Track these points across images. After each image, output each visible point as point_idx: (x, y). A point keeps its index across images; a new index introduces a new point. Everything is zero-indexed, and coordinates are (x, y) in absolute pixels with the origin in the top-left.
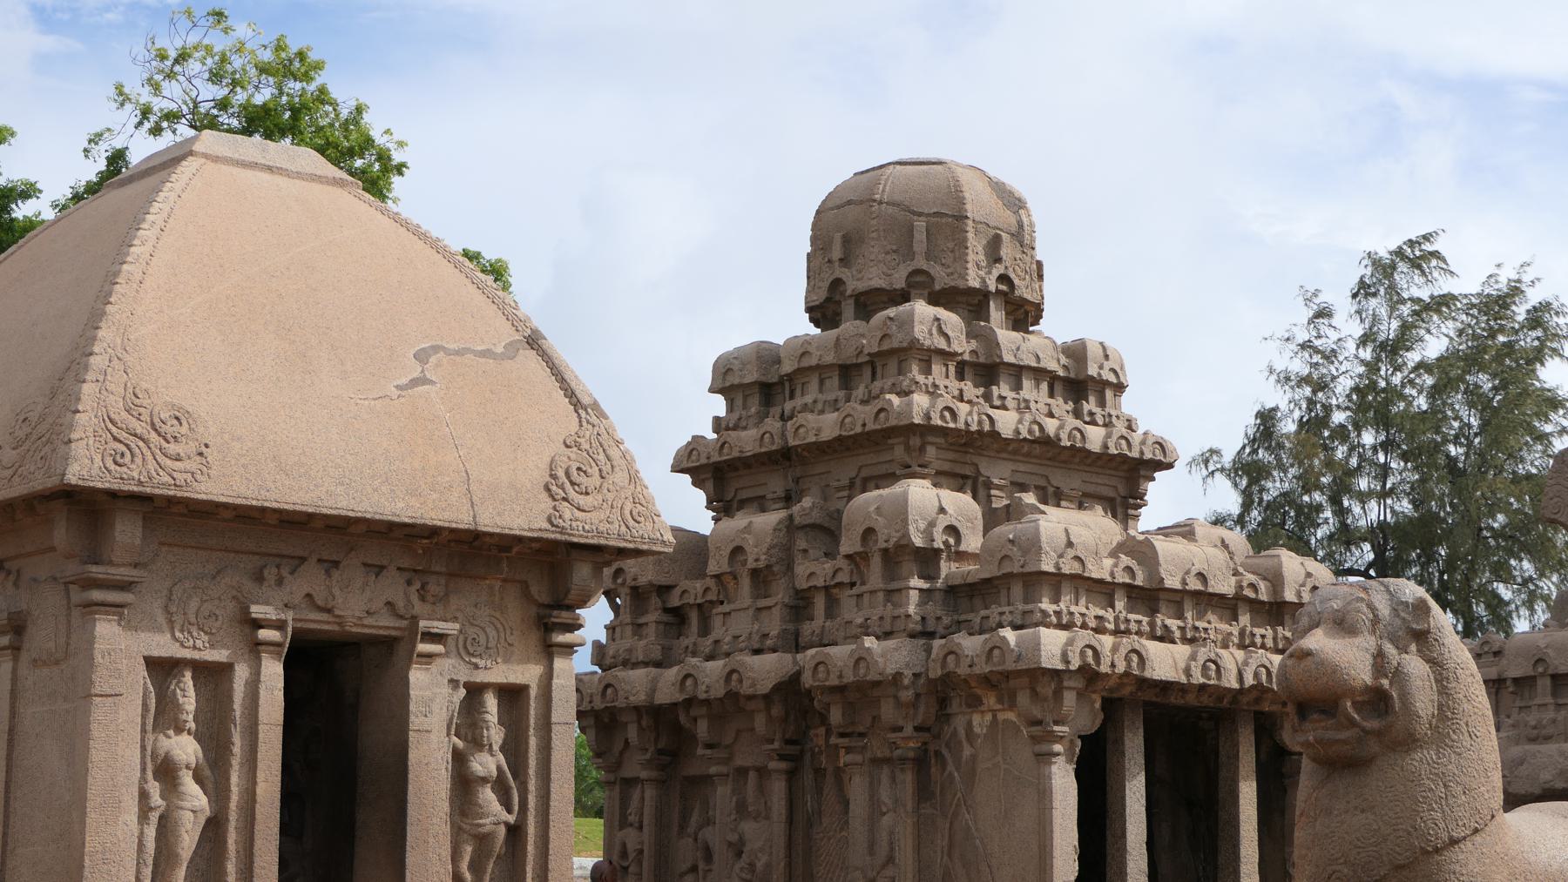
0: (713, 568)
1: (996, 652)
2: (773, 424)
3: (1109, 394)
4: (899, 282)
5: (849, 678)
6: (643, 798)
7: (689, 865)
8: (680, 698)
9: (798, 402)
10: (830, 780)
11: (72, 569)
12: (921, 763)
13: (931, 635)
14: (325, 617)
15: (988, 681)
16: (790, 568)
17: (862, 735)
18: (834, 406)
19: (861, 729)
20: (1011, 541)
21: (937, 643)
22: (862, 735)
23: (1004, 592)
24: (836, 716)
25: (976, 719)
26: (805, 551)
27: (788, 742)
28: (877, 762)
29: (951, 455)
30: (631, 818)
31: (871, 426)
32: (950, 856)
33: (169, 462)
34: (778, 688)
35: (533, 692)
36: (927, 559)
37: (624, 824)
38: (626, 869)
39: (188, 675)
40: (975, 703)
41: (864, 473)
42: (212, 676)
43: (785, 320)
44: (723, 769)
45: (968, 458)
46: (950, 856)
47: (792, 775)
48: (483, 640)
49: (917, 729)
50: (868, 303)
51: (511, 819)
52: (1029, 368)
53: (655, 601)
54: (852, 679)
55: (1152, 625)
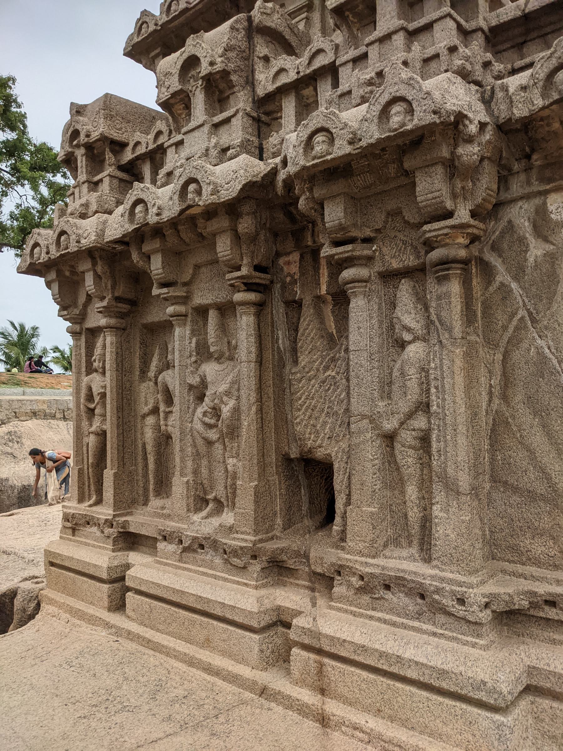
6: (104, 346)
7: (150, 406)
8: (130, 228)
17: (367, 240)
19: (368, 233)
22: (367, 240)
24: (334, 214)
26: (266, 59)
28: (390, 277)
30: (96, 364)
32: (505, 397)
37: (90, 370)
38: (93, 410)
44: (181, 309)
46: (505, 397)
47: (260, 308)
49: (474, 214)
53: (109, 156)
54: (377, 135)
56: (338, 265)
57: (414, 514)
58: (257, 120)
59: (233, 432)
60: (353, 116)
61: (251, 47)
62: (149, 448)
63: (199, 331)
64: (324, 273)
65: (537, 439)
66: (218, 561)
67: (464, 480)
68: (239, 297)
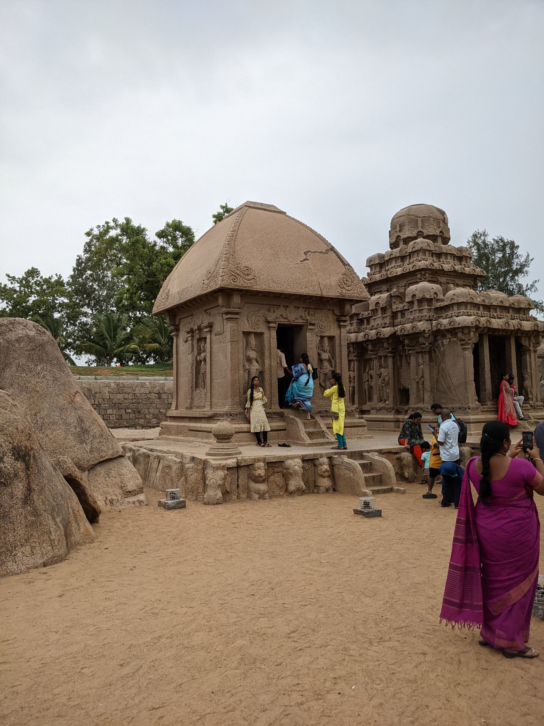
0: (371, 308)
1: (452, 323)
2: (383, 272)
3: (468, 259)
4: (414, 234)
5: (411, 332)
6: (354, 365)
9: (390, 266)
10: (404, 358)
11: (224, 310)
12: (430, 353)
13: (431, 320)
14: (286, 320)
15: (448, 331)
16: (391, 307)
17: (414, 346)
18: (400, 266)
20: (454, 295)
21: (434, 323)
23: (451, 308)
24: (406, 342)
25: (445, 341)
27: (393, 349)
28: (418, 353)
29: (431, 276)
31: (411, 270)
33: (246, 281)
34: (390, 336)
35: (337, 338)
36: (429, 301)
39: (253, 335)
40: (444, 336)
41: (408, 282)
42: (259, 335)
43: (384, 248)
44: (375, 356)
45: (435, 277)
47: (394, 357)
48: (323, 325)
49: (429, 344)
50: (407, 241)
51: (332, 369)
52: (449, 254)
53: (355, 317)
55: (490, 315)
56: (409, 350)
57: (422, 396)
58: (393, 316)
59: (388, 384)
60: (408, 326)
61: (391, 300)
62: (366, 390)
63: (380, 361)
64: (407, 351)
65: (443, 382)
66: (385, 411)
67: (429, 389)
68: (389, 355)
